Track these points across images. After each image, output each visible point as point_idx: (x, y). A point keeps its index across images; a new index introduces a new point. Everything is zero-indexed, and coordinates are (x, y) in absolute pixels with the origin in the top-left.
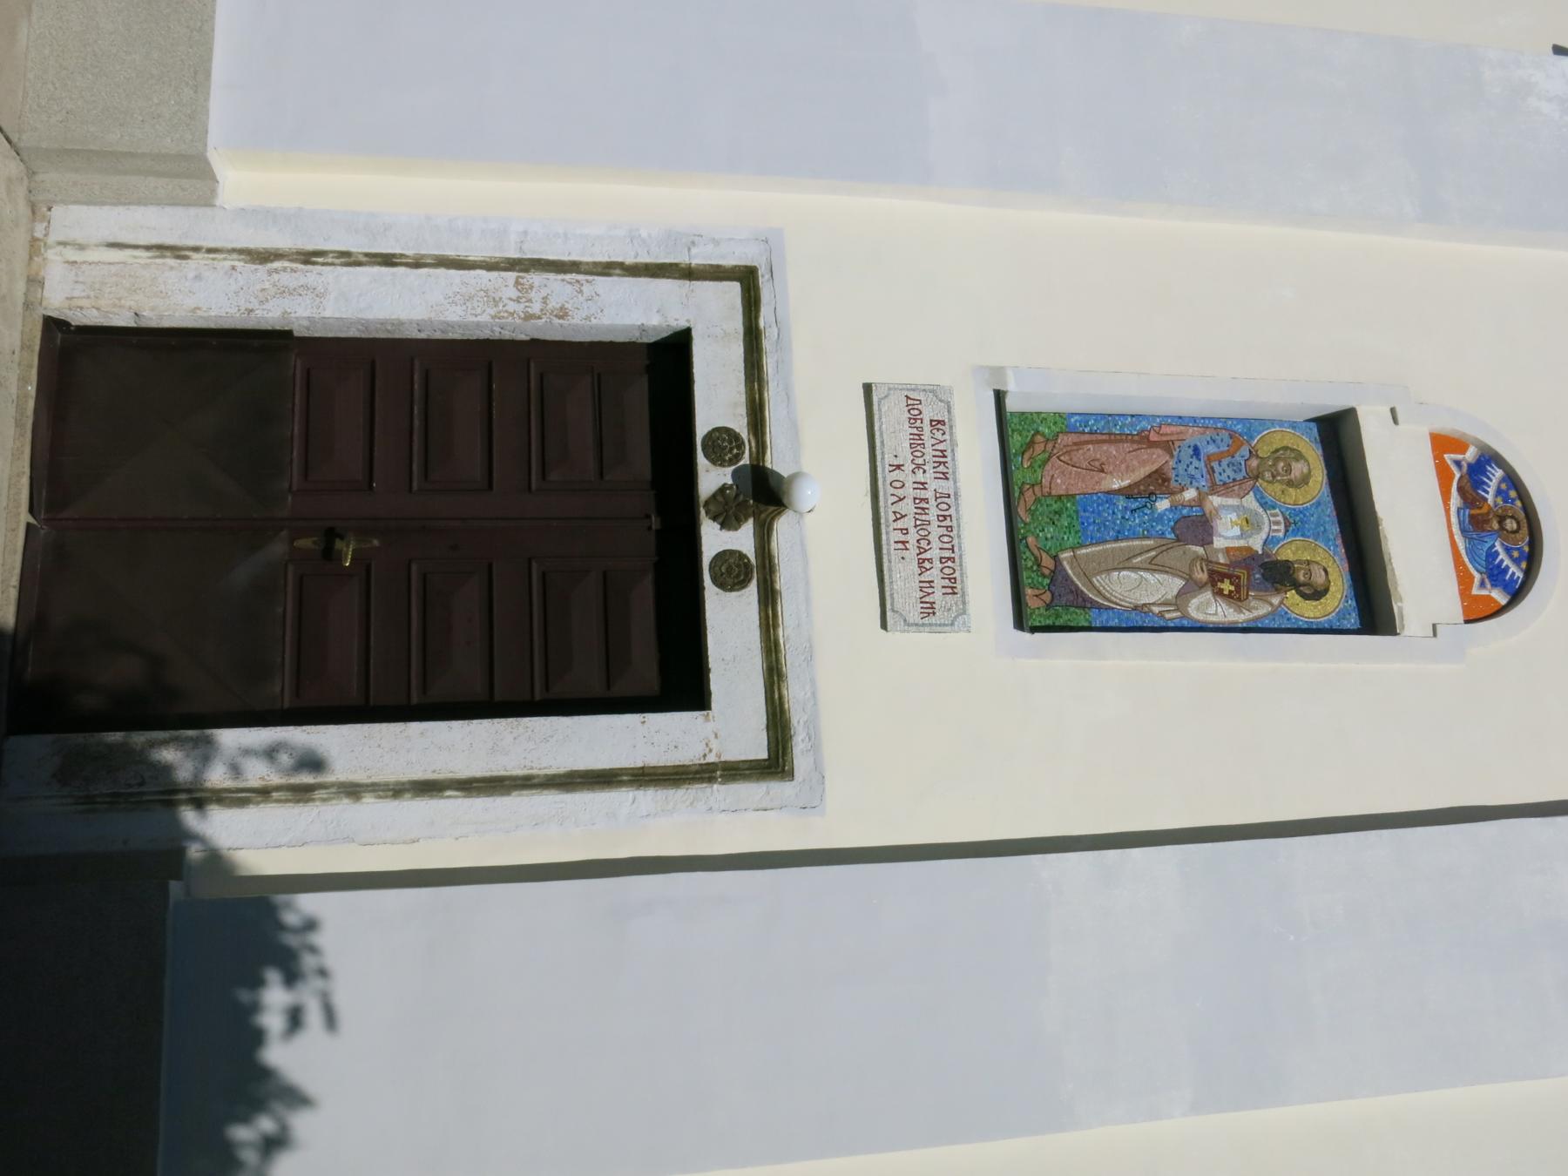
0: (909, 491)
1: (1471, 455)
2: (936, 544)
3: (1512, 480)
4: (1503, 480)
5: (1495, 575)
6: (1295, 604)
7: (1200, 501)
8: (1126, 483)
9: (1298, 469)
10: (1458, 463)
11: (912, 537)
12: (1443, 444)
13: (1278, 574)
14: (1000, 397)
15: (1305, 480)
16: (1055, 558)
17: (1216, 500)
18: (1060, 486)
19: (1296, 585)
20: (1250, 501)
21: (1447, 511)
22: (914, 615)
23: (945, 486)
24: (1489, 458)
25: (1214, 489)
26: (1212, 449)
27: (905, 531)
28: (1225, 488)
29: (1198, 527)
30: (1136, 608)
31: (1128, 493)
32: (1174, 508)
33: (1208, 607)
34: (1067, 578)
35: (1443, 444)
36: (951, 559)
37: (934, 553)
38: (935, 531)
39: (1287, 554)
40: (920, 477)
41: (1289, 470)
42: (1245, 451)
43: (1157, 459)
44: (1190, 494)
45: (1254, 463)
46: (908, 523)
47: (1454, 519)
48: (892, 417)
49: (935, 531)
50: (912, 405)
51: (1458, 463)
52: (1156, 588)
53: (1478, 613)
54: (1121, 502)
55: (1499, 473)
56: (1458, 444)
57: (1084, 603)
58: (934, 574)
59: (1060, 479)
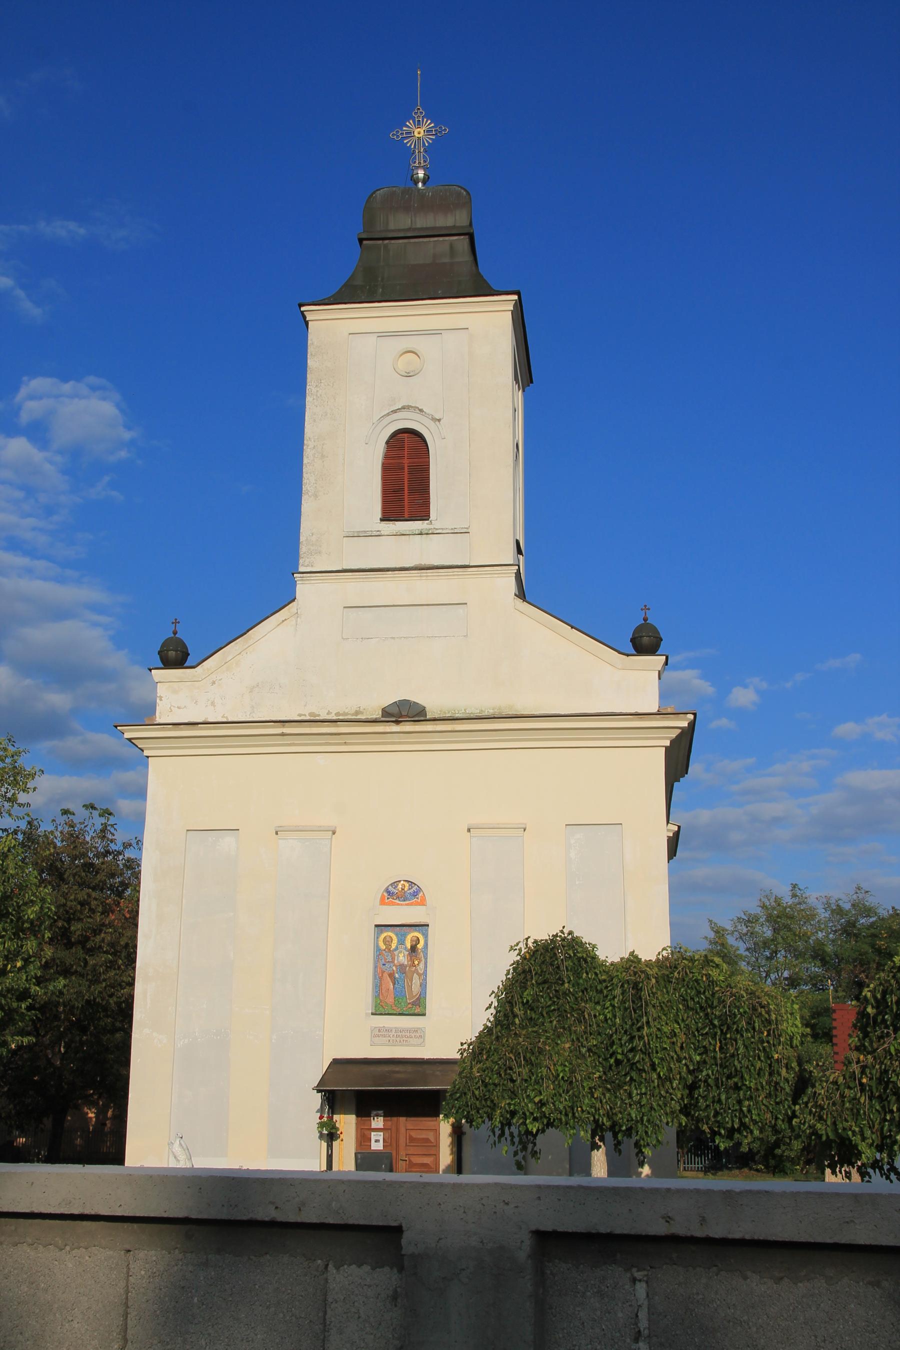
0: (394, 1039)
1: (386, 894)
2: (406, 1034)
3: (391, 885)
4: (392, 886)
5: (415, 894)
6: (420, 946)
7: (396, 966)
8: (392, 984)
9: (388, 939)
10: (388, 898)
11: (405, 1039)
12: (382, 902)
13: (413, 949)
14: (372, 1014)
15: (391, 937)
16: (409, 1004)
17: (396, 962)
18: (392, 1000)
19: (416, 945)
20: (396, 953)
21: (398, 904)
22: (421, 1040)
23: (394, 1031)
24: (387, 891)
25: (393, 962)
26: (383, 961)
27: (403, 1041)
28: (393, 959)
29: (402, 967)
30: (421, 986)
31: (394, 984)
32: (397, 973)
33: (422, 965)
34: (413, 1002)
35: (382, 902)
36: (409, 1030)
37: (408, 1034)
38: (403, 1034)
39: (409, 946)
40: (391, 1036)
41: (389, 941)
42: (384, 952)
43: (386, 975)
44: (394, 968)
45: (387, 950)
46: (402, 1040)
47: (402, 903)
48: (376, 1040)
49: (403, 1034)
50: (375, 1036)
51: (388, 898)
52: (416, 980)
53: (423, 903)
54: (396, 986)
55: (390, 887)
56: (383, 896)
57: (419, 999)
58: (413, 1035)
59: (390, 1000)
